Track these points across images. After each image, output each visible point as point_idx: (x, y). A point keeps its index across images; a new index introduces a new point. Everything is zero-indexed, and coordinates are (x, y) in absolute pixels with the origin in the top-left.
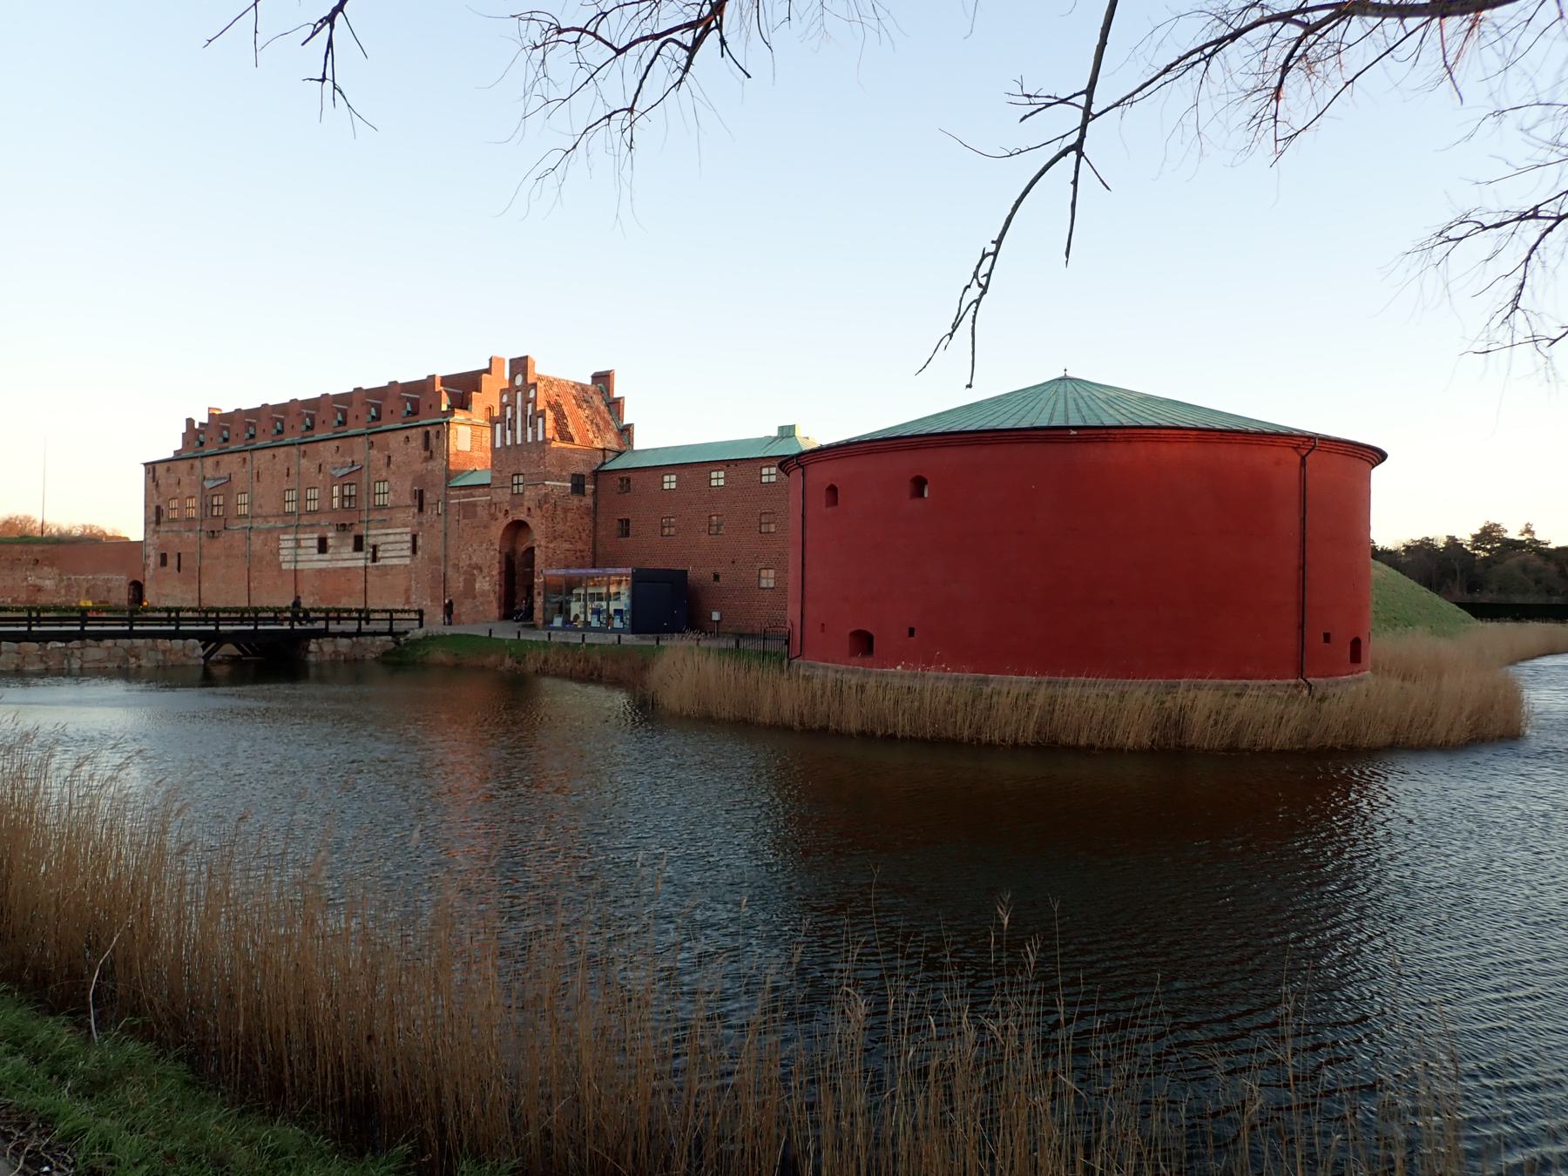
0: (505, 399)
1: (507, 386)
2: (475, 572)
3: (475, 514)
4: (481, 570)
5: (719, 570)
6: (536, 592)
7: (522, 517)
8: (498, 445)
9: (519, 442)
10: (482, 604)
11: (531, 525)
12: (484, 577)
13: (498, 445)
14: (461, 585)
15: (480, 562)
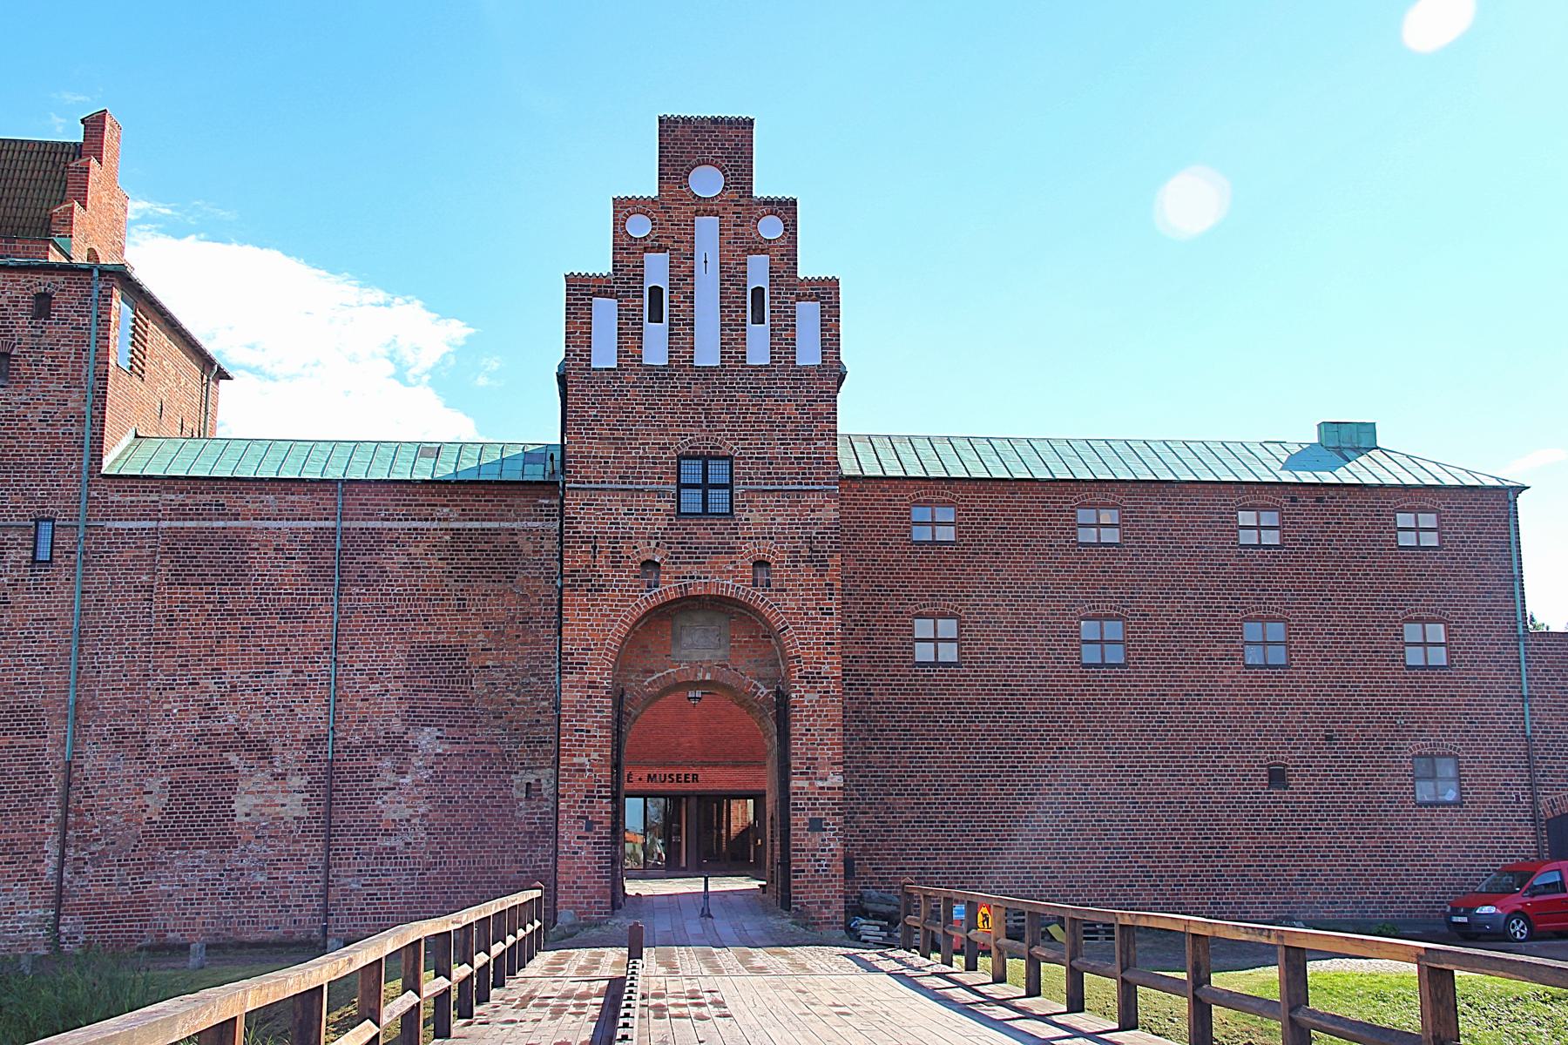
0: (640, 227)
1: (648, 187)
2: (233, 758)
3: (236, 574)
4: (261, 751)
5: (1282, 757)
6: (799, 820)
7: (729, 586)
8: (604, 355)
9: (707, 353)
10: (263, 865)
11: (776, 619)
12: (283, 776)
13: (604, 355)
14: (155, 805)
15: (257, 723)
